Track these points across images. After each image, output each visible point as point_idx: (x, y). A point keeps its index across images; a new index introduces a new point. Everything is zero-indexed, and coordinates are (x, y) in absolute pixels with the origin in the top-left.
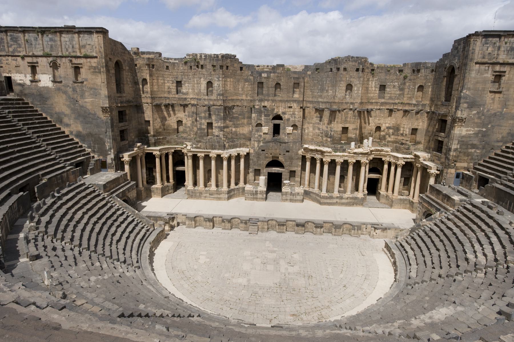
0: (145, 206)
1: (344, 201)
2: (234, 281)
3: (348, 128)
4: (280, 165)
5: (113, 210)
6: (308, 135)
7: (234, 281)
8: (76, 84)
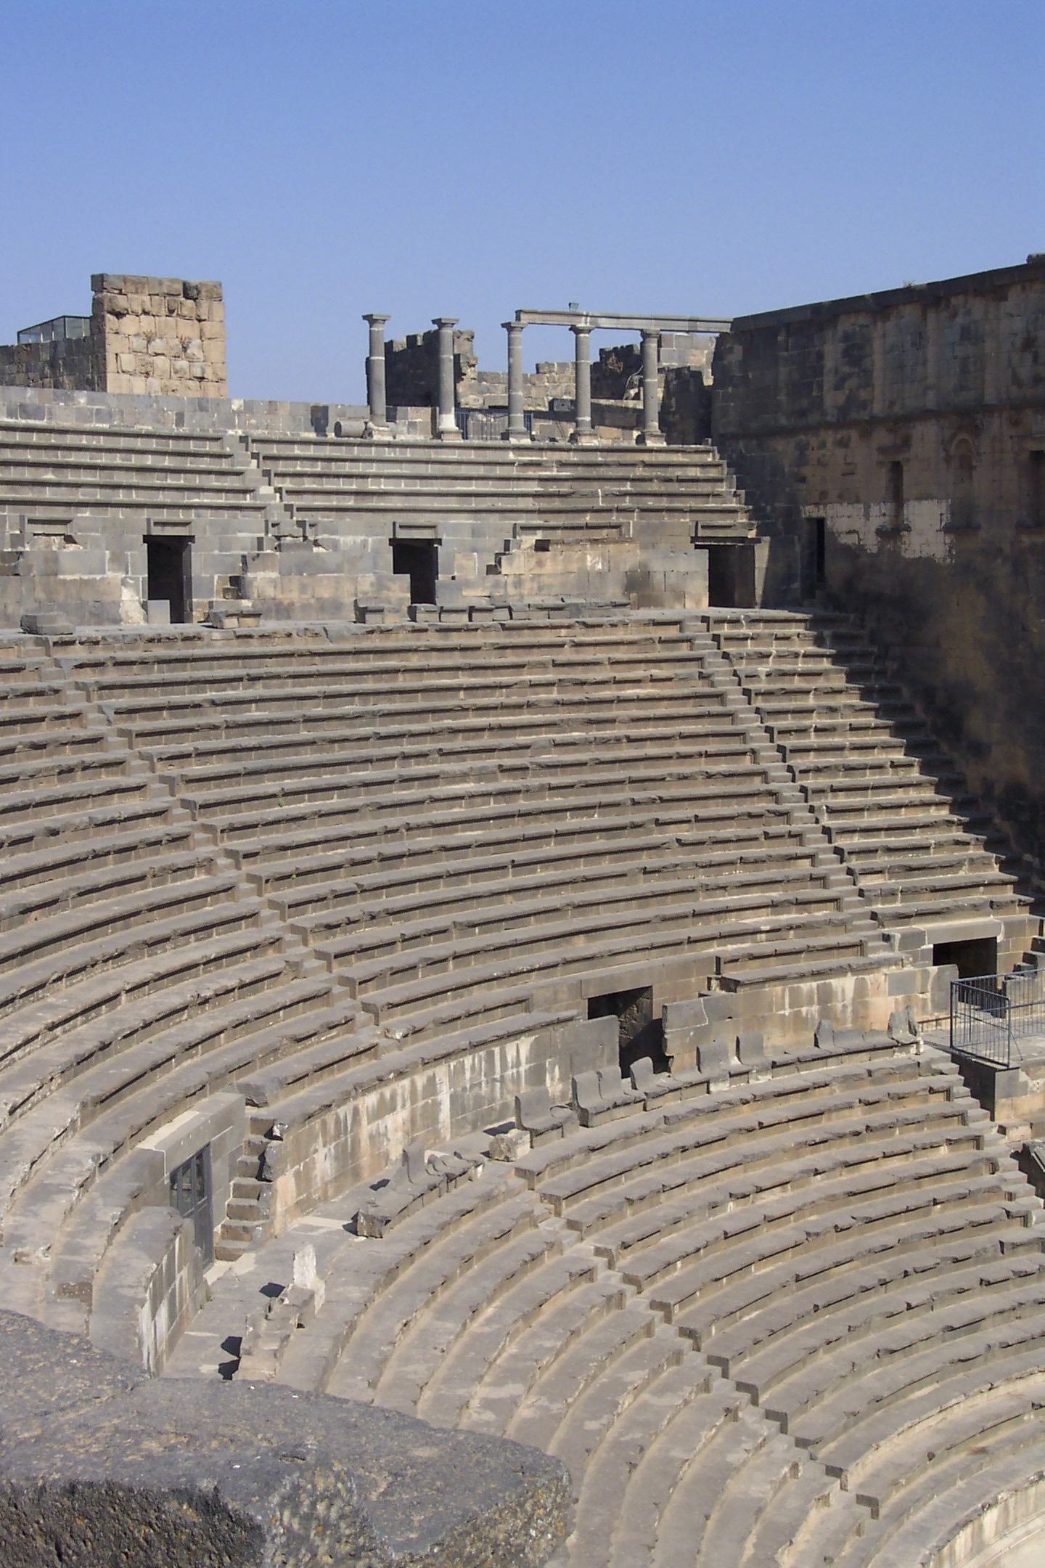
8: (1026, 540)
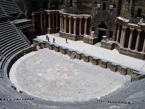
0: (37, 37)
1: (132, 54)
2: (38, 74)
3: (141, 9)
4: (105, 27)
5: (16, 34)
6: (122, 10)
7: (38, 74)
